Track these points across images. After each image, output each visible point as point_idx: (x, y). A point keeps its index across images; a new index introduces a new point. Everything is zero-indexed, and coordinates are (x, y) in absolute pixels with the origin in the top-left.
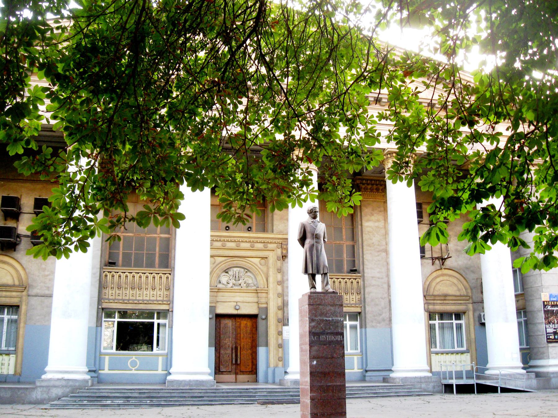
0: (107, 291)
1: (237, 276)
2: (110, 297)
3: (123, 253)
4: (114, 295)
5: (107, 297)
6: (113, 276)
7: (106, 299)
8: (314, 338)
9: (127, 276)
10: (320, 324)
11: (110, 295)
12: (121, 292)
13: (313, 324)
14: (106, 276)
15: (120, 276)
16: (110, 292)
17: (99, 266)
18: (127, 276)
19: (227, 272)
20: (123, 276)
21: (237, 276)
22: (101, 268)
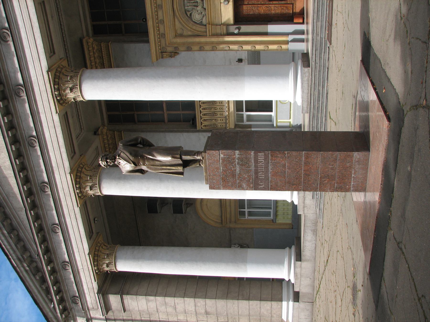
0: (219, 125)
1: (194, 4)
2: (224, 121)
3: (183, 110)
4: (222, 119)
5: (224, 124)
6: (205, 120)
7: (226, 125)
8: (261, 185)
9: (204, 109)
10: (245, 178)
11: (222, 122)
12: (219, 113)
13: (244, 185)
14: (205, 126)
15: (204, 115)
16: (219, 121)
17: (197, 134)
18: (204, 109)
19: (191, 15)
20: (204, 112)
21: (194, 4)
22: (199, 131)
